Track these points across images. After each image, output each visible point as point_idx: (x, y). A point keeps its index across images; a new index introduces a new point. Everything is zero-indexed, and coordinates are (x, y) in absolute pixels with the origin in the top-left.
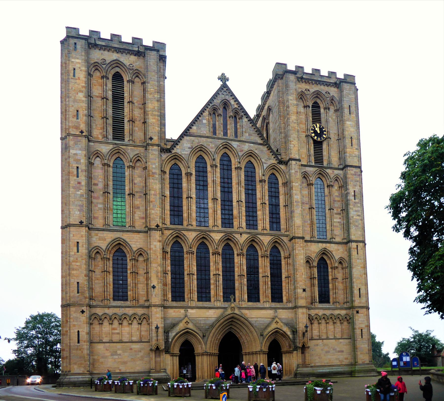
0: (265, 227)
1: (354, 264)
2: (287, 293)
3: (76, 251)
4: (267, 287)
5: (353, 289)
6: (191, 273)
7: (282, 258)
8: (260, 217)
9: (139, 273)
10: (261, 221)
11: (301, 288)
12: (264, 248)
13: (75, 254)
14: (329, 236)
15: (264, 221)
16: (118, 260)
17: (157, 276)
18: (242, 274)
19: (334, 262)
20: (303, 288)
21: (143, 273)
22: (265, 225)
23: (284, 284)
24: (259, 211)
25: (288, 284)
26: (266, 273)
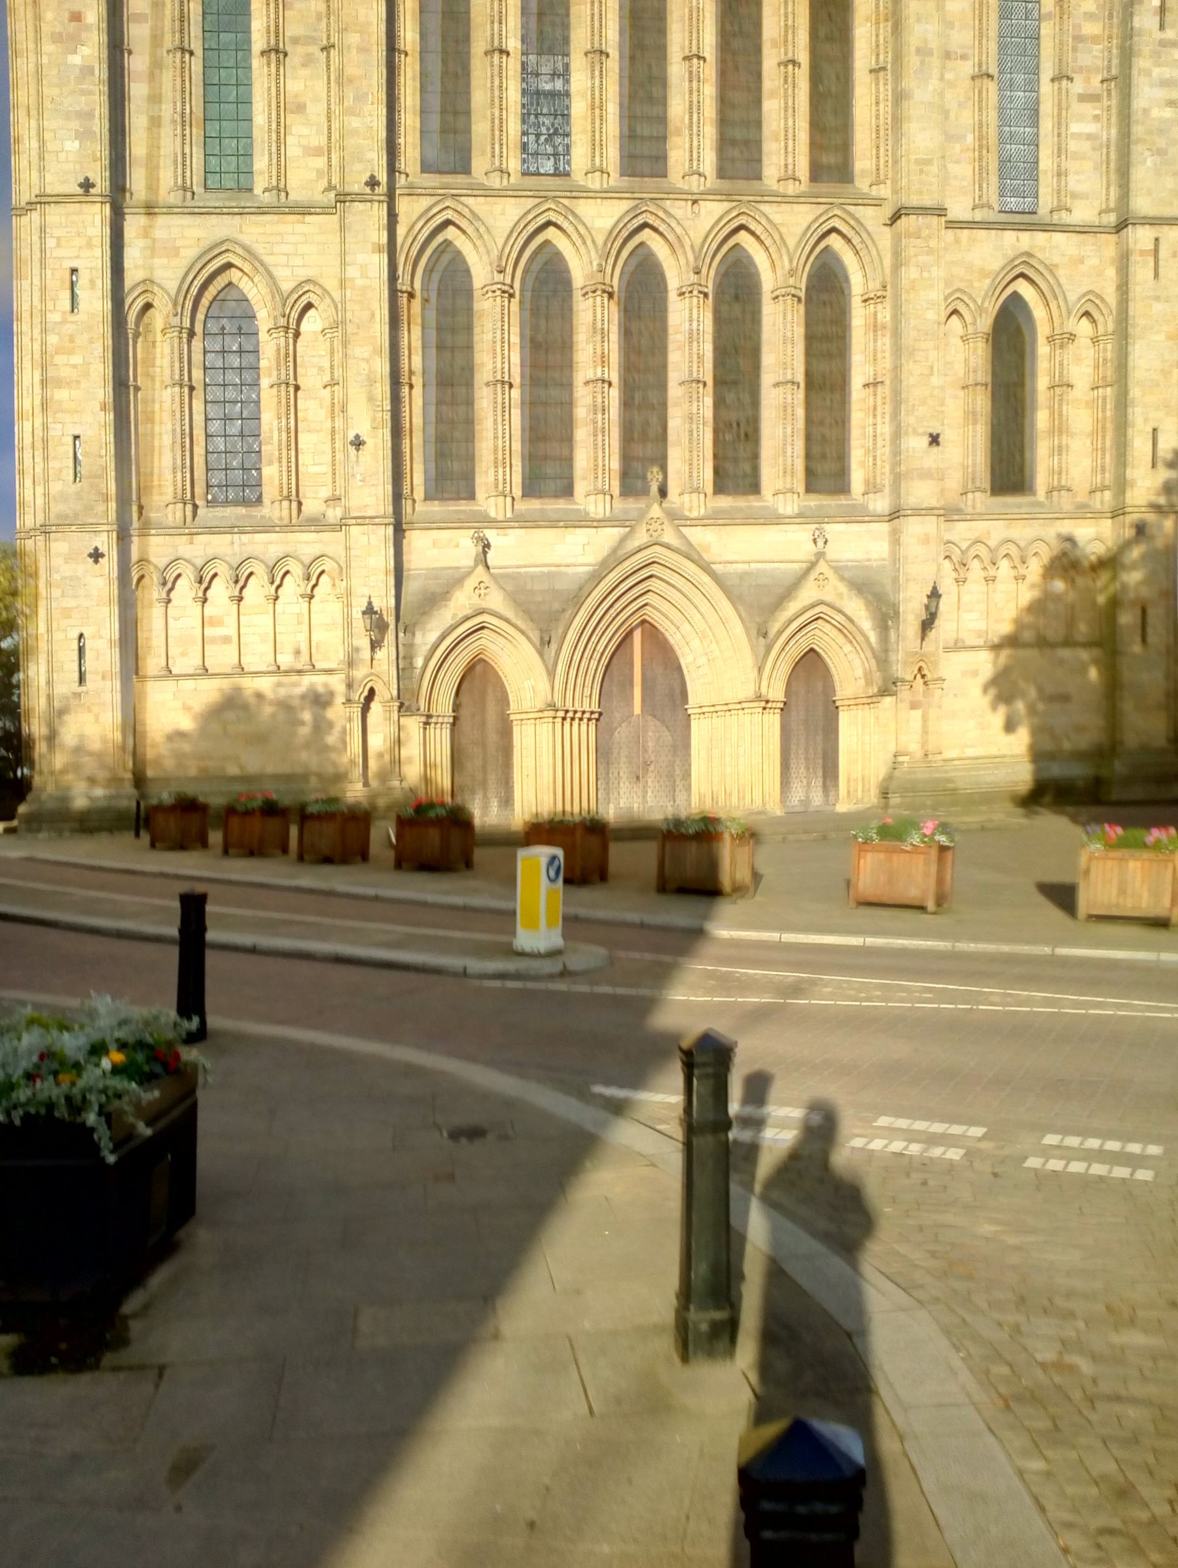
0: (790, 167)
1: (1141, 322)
2: (867, 452)
3: (68, 307)
4: (789, 430)
5: (1130, 431)
6: (499, 377)
7: (856, 302)
8: (775, 124)
9: (302, 386)
10: (777, 140)
11: (921, 430)
12: (786, 262)
13: (64, 322)
14: (1044, 209)
15: (790, 142)
16: (223, 334)
17: (371, 399)
18: (695, 375)
19: (1061, 315)
20: (931, 430)
21: (320, 385)
22: (790, 160)
23: (857, 416)
24: (773, 94)
25: (875, 416)
26: (789, 371)
